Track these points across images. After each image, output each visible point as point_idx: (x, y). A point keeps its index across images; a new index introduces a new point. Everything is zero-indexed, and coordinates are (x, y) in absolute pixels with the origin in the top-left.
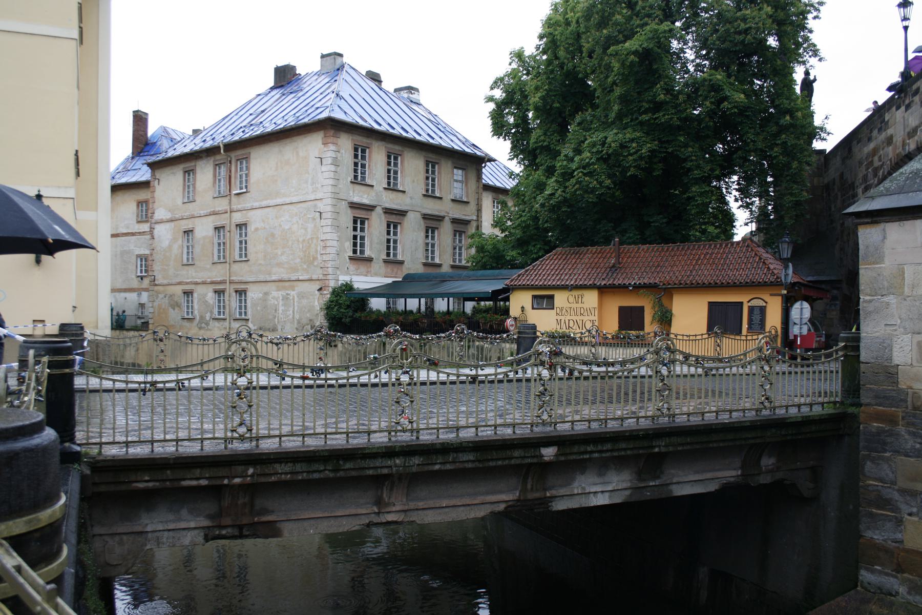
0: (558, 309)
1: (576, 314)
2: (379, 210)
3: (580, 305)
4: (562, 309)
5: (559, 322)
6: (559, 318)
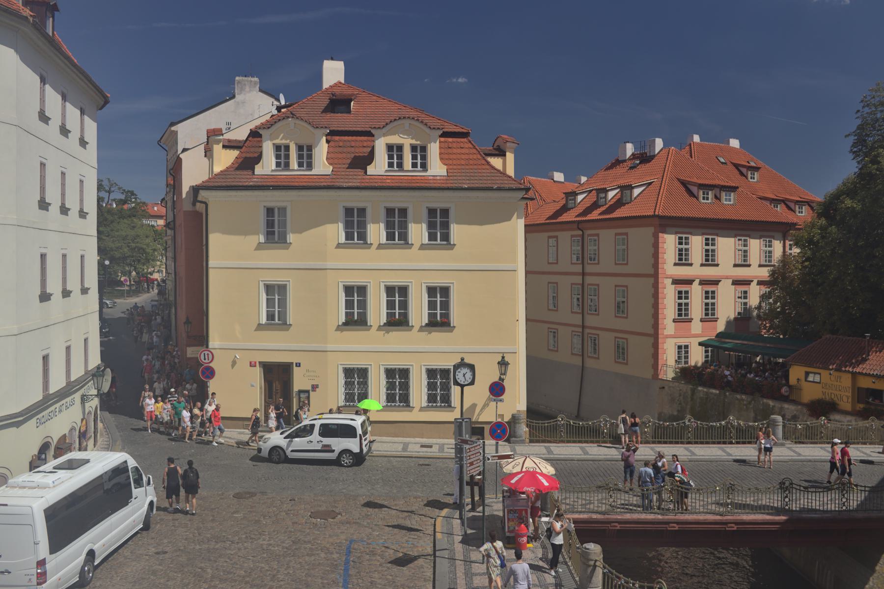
1: (836, 390)
3: (838, 383)
4: (826, 384)
5: (824, 393)
6: (824, 390)
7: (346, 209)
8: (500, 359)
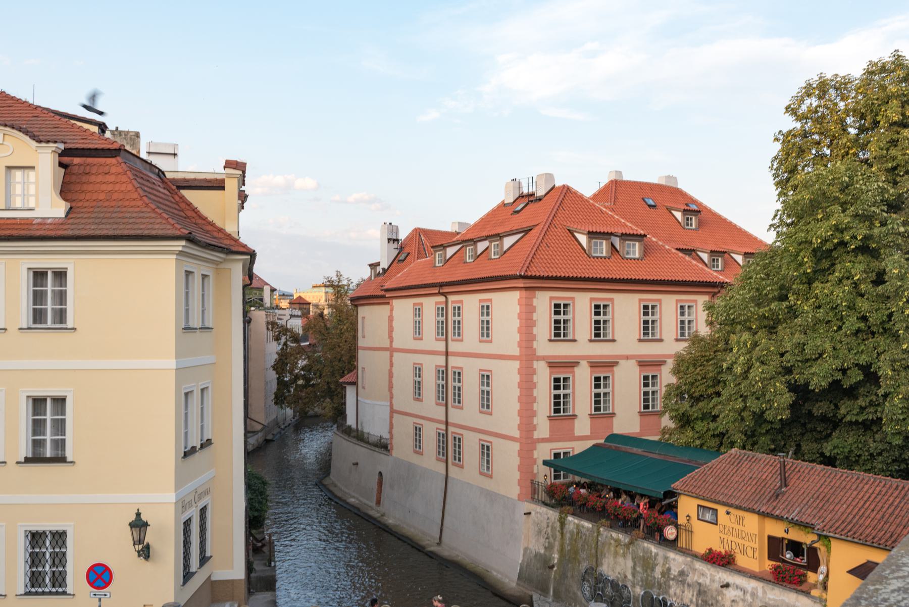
0: (721, 526)
1: (738, 536)
2: (584, 364)
3: (741, 527)
4: (724, 527)
6: (723, 536)
7: (34, 273)
8: (133, 517)
